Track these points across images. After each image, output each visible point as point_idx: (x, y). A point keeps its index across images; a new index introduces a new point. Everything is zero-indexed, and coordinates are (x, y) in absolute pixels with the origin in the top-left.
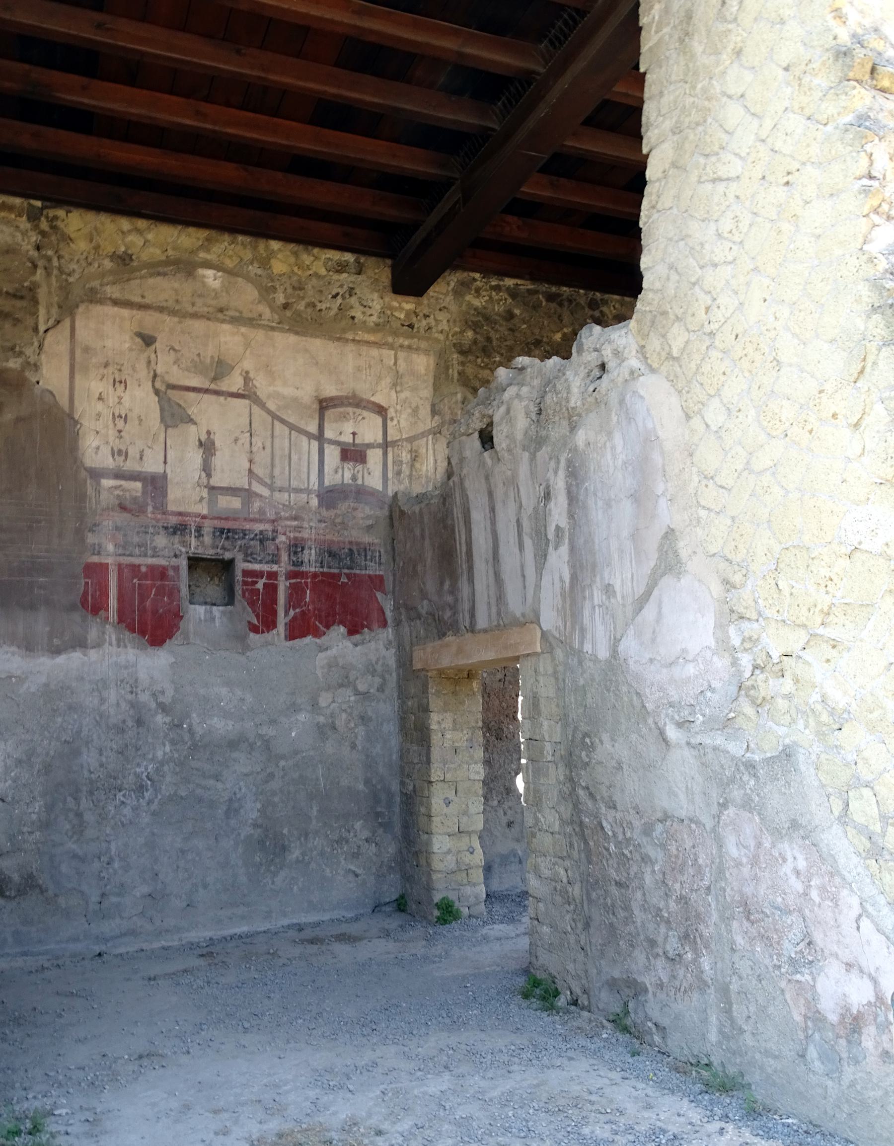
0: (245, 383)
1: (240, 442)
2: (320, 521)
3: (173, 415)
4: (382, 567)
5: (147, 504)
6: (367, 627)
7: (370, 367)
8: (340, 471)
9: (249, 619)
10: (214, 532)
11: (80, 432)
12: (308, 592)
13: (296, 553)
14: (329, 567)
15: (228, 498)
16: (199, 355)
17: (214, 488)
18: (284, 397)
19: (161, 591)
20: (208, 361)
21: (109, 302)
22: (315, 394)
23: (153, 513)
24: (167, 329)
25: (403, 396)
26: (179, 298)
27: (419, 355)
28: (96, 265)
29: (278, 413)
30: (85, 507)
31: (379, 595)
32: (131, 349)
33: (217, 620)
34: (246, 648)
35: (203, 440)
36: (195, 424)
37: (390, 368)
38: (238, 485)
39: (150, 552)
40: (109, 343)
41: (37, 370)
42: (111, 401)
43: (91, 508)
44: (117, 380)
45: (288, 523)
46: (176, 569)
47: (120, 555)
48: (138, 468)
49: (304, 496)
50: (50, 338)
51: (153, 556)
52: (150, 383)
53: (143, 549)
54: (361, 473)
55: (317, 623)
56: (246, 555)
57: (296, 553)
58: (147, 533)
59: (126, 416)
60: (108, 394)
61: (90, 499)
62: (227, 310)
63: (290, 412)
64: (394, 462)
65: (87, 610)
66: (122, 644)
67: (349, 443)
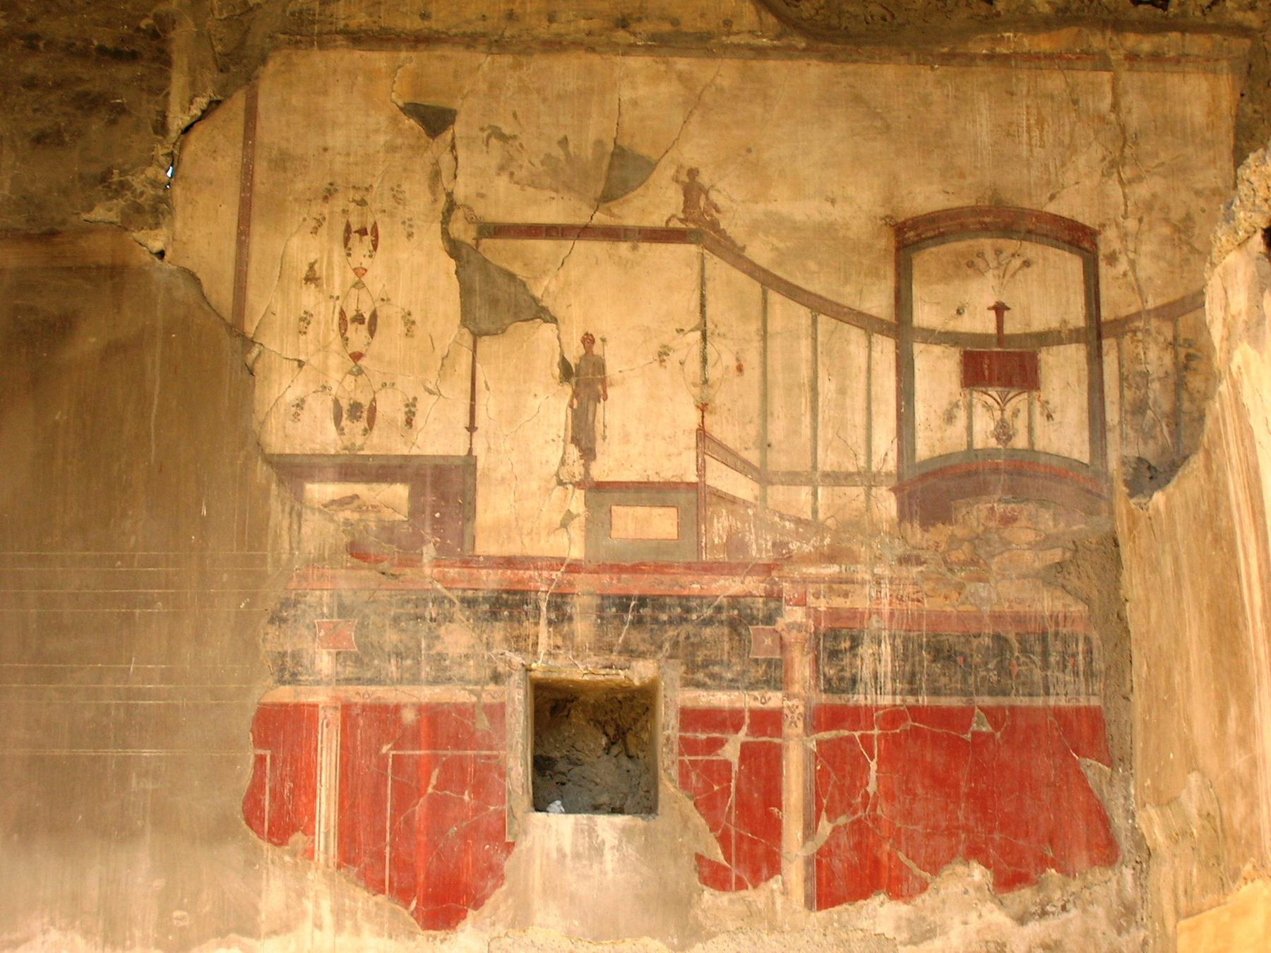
0: (685, 202)
1: (674, 358)
2: (904, 560)
3: (494, 302)
4: (1098, 686)
5: (423, 542)
6: (1053, 864)
7: (1041, 122)
8: (961, 415)
9: (700, 849)
10: (601, 609)
11: (258, 368)
12: (873, 765)
13: (834, 654)
14: (935, 692)
15: (640, 511)
16: (564, 142)
17: (600, 487)
18: (795, 227)
19: (455, 774)
20: (588, 153)
21: (340, 40)
22: (881, 212)
24: (483, 87)
25: (1142, 191)
26: (517, 8)
27: (1184, 73)
29: (779, 273)
30: (263, 559)
31: (1092, 768)
32: (391, 149)
33: (610, 859)
34: (695, 932)
35: (573, 359)
36: (554, 320)
37: (1102, 119)
38: (668, 474)
39: (426, 670)
40: (337, 139)
41: (157, 225)
43: (277, 561)
44: (354, 227)
45: (812, 570)
46: (497, 712)
47: (348, 681)
48: (399, 448)
49: (857, 492)
50: (195, 143)
51: (435, 682)
52: (437, 227)
53: (409, 662)
54: (1023, 415)
55: (902, 856)
56: (692, 667)
57: (834, 654)
58: (419, 618)
59: (374, 316)
60: (330, 264)
61: (277, 537)
62: (639, 20)
63: (812, 265)
64: (1122, 378)
65: (260, 833)
66: (348, 923)
67: (986, 337)
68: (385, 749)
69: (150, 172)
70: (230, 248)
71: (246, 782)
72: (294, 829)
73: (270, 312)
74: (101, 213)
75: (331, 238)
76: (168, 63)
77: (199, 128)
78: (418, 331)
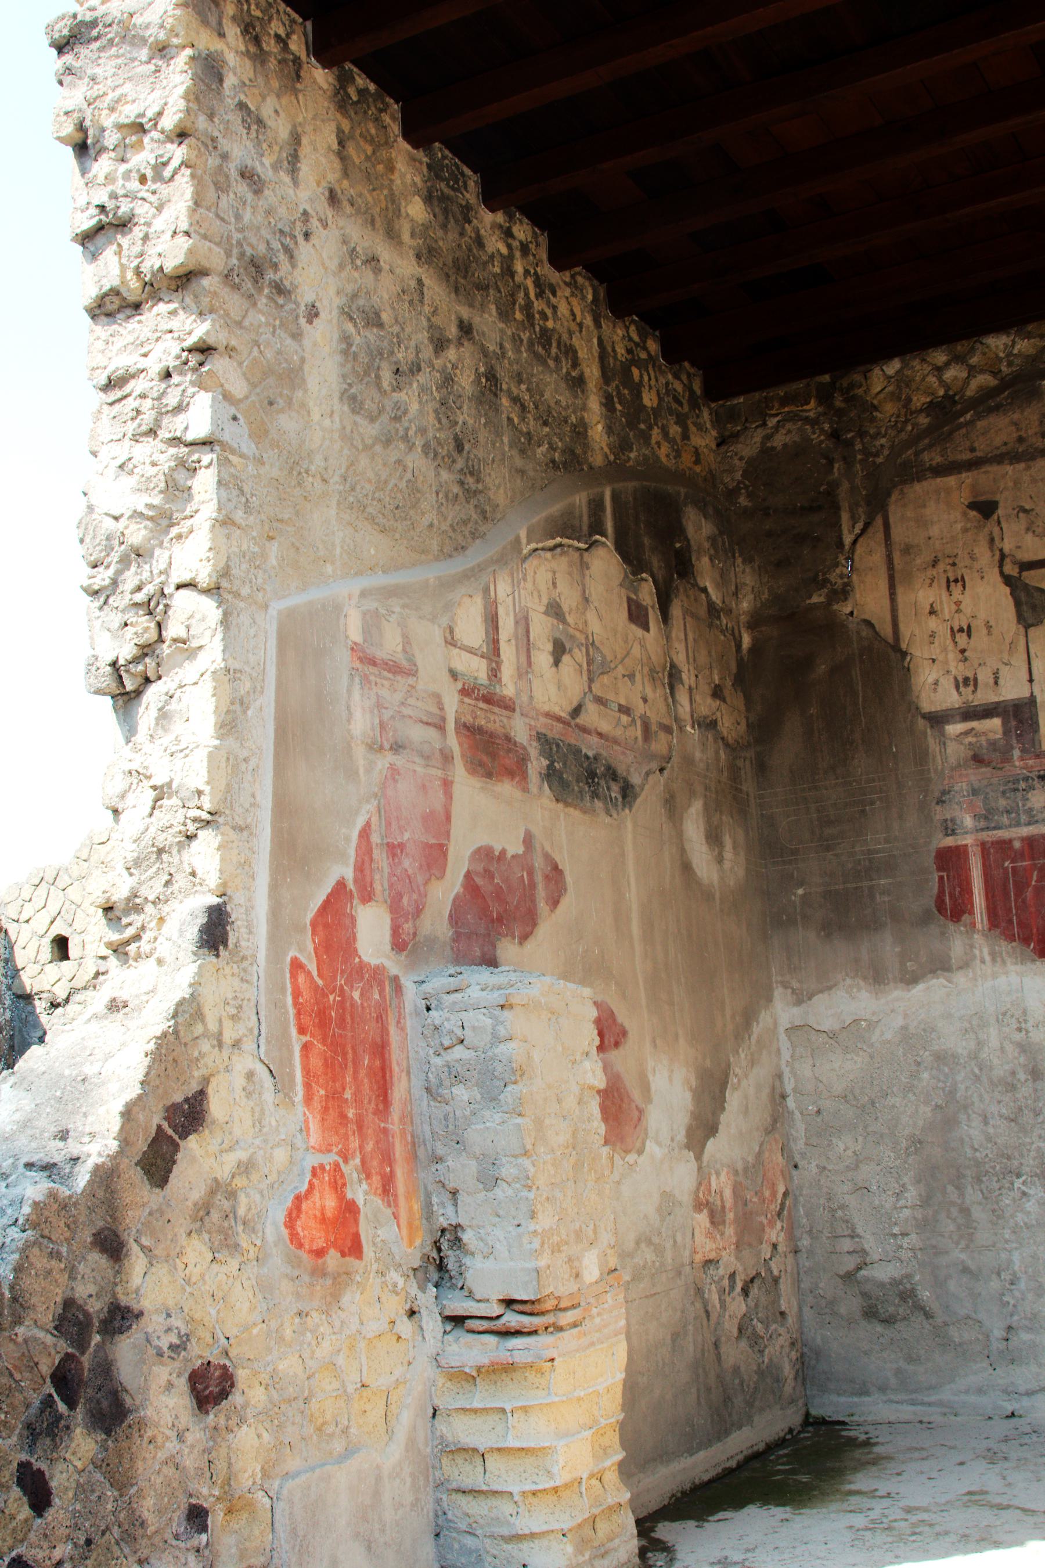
3: (1034, 607)
5: (1012, 748)
23: (1022, 759)
24: (1011, 484)
26: (1022, 433)
28: (909, 428)
32: (965, 530)
39: (1024, 818)
41: (846, 599)
42: (946, 611)
43: (936, 770)
47: (982, 830)
50: (859, 550)
51: (1029, 824)
52: (996, 570)
58: (1016, 790)
59: (969, 627)
60: (941, 602)
61: (934, 757)
65: (945, 916)
68: (1006, 864)
69: (838, 571)
70: (886, 602)
71: (935, 891)
72: (963, 912)
73: (913, 635)
74: (816, 599)
75: (939, 587)
76: (839, 508)
77: (861, 540)
78: (994, 631)
